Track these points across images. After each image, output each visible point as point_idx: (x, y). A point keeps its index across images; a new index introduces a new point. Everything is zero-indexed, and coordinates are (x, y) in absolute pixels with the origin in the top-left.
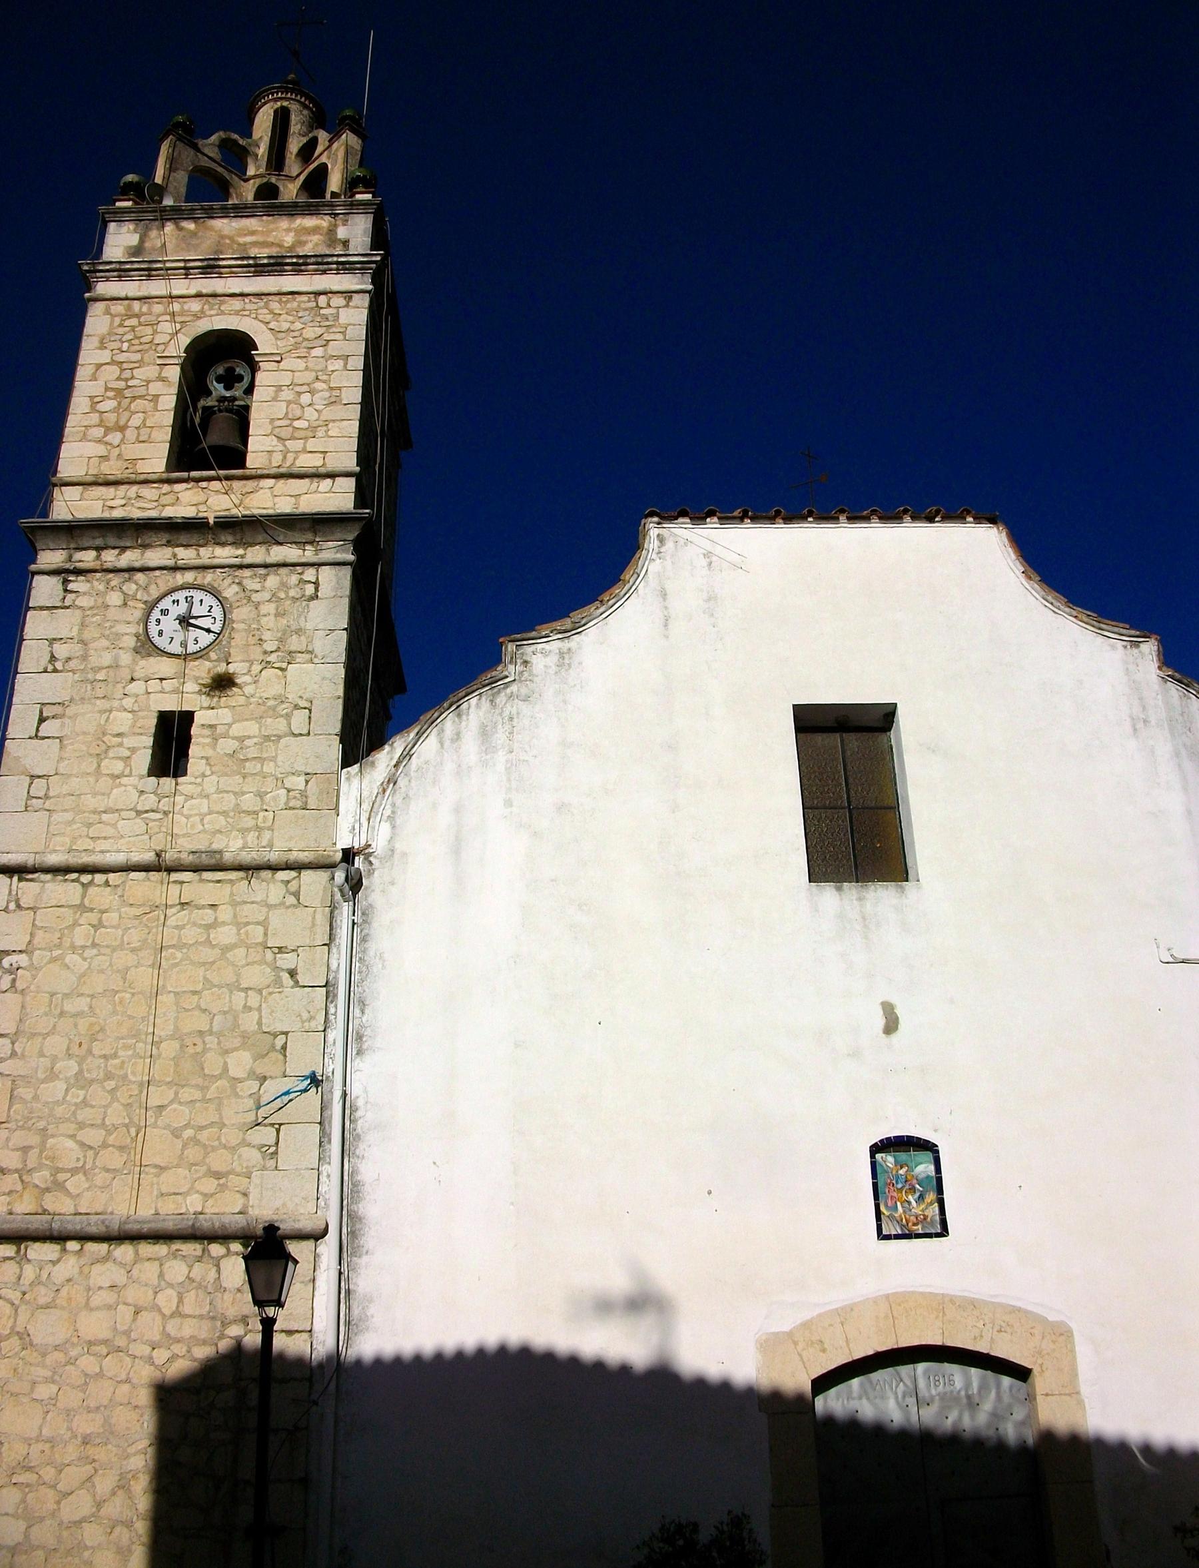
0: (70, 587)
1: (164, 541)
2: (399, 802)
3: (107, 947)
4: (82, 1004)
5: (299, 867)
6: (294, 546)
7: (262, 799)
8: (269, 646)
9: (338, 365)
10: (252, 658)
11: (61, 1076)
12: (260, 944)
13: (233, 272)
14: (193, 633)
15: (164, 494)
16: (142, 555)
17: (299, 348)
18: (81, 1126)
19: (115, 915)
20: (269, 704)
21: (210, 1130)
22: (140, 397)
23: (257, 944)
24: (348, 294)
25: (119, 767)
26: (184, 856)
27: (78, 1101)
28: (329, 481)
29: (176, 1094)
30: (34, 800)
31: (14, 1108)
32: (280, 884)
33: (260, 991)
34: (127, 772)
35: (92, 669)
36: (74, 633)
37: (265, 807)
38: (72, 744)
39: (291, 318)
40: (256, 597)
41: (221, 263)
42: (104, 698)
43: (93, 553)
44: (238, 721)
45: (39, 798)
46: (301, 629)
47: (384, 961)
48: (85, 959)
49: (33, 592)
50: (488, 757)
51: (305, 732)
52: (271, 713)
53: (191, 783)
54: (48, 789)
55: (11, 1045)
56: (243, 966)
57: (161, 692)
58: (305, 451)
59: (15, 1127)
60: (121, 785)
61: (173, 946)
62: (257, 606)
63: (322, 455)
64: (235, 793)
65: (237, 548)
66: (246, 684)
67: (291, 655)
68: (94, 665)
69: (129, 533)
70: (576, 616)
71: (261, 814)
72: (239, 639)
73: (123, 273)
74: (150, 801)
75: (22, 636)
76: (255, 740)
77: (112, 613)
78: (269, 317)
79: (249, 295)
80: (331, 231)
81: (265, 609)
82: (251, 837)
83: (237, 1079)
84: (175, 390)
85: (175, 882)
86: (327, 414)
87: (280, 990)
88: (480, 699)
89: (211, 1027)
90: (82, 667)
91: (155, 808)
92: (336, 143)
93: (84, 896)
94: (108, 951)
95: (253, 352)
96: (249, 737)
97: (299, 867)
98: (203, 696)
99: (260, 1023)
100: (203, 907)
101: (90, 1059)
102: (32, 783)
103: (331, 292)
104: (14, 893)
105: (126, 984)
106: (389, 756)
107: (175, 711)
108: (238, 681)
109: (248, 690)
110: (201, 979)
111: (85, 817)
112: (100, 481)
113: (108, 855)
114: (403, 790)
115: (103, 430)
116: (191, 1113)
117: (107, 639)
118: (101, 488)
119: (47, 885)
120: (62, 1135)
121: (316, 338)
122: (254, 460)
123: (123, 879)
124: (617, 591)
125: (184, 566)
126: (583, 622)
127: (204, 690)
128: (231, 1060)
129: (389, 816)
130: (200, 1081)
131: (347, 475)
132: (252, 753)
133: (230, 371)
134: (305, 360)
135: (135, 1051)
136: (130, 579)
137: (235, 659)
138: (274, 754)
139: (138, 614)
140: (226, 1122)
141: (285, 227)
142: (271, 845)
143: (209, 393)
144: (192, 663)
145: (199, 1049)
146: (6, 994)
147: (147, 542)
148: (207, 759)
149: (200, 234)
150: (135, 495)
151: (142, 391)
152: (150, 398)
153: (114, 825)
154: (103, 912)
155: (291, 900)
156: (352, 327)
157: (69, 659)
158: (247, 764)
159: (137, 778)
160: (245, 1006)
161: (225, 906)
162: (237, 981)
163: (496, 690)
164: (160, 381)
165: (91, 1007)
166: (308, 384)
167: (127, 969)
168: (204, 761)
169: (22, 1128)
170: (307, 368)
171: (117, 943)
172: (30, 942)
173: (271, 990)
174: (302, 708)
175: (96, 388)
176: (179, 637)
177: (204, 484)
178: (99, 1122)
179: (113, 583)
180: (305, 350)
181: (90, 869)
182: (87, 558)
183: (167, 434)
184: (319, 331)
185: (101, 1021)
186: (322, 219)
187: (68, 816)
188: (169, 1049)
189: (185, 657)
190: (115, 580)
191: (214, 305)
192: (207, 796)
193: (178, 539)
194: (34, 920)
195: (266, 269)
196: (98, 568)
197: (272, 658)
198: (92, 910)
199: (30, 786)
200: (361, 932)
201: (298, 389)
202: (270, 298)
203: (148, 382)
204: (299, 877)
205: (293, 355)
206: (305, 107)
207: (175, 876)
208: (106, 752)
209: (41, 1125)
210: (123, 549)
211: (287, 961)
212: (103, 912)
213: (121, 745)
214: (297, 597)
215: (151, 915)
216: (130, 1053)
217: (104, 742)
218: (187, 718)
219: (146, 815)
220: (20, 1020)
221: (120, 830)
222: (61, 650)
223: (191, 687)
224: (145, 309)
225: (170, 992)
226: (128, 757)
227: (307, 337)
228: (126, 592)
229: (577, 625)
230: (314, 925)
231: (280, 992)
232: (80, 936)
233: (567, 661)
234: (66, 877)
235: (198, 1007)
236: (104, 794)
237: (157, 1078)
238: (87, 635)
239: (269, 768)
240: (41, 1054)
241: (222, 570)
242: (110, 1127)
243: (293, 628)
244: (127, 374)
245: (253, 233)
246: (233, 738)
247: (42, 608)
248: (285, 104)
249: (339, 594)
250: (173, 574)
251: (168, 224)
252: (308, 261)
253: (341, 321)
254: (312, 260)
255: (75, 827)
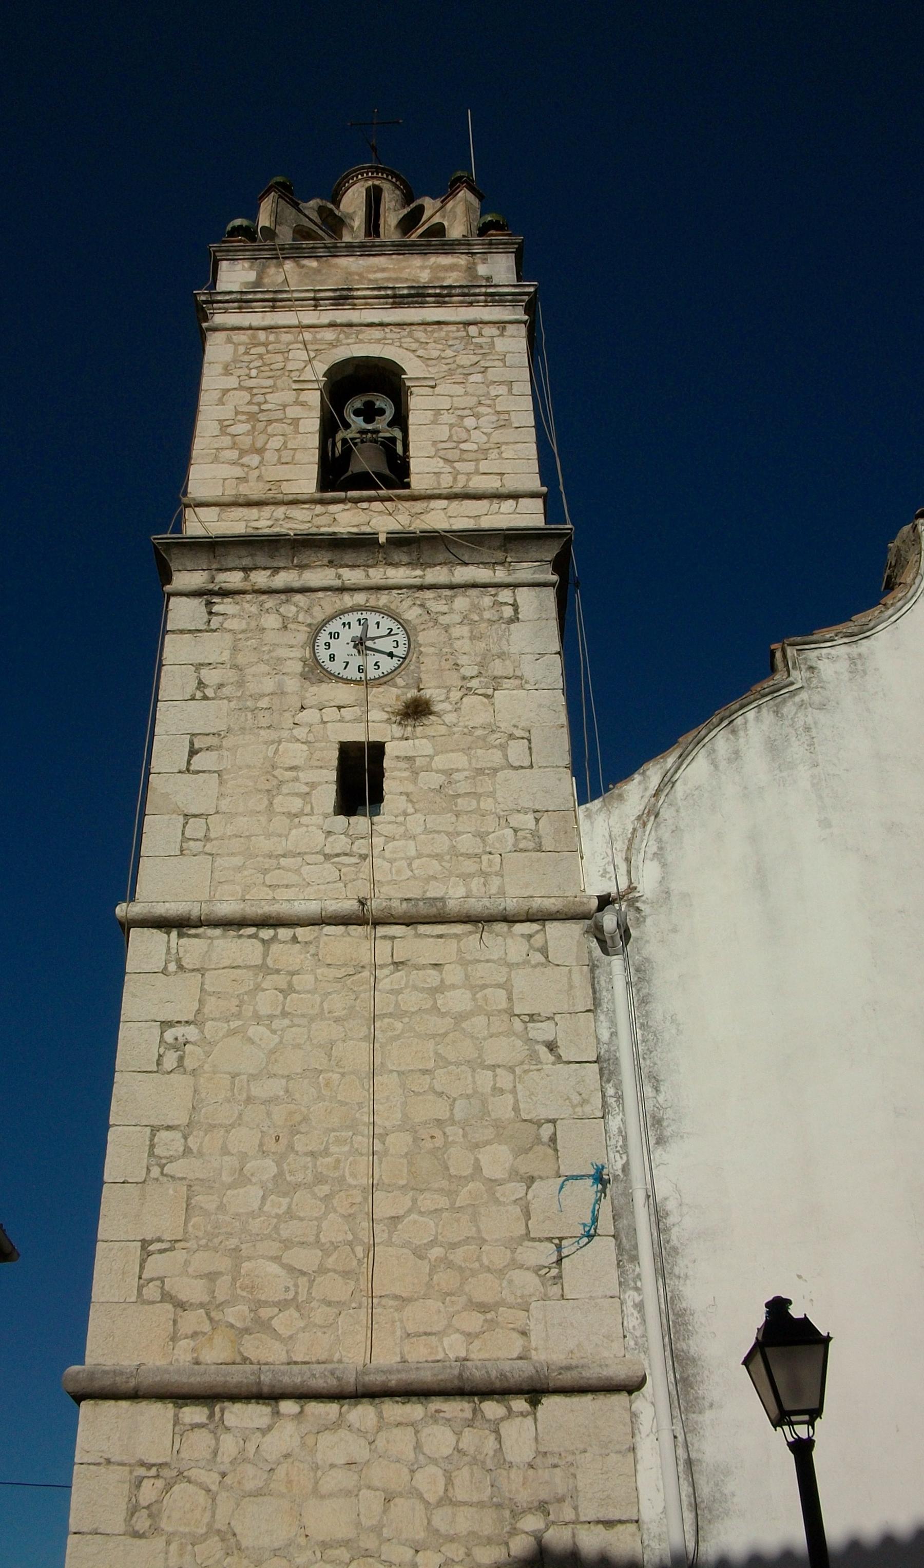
0: (215, 609)
1: (325, 561)
2: (666, 836)
3: (303, 1016)
4: (275, 1087)
5: (541, 918)
6: (481, 566)
7: (484, 841)
8: (469, 671)
9: (503, 390)
10: (448, 684)
11: (254, 1180)
12: (505, 1011)
13: (368, 302)
14: (372, 658)
15: (317, 516)
16: (300, 576)
17: (454, 374)
18: (287, 1244)
19: (310, 978)
20: (476, 734)
21: (466, 1247)
22: (276, 421)
23: (499, 1011)
24: (501, 325)
25: (296, 804)
26: (395, 904)
27: (281, 1212)
28: (511, 502)
29: (414, 1201)
30: (191, 843)
31: (194, 1220)
32: (520, 939)
33: (511, 1070)
34: (307, 809)
35: (251, 696)
36: (226, 657)
37: (488, 849)
38: (233, 779)
39: (440, 347)
40: (443, 620)
41: (355, 293)
42: (269, 728)
43: (240, 575)
44: (442, 752)
45: (197, 840)
46: (504, 653)
47: (678, 1025)
48: (274, 1032)
49: (170, 615)
50: (785, 774)
51: (526, 763)
52: (481, 743)
53: (390, 823)
54: (208, 829)
55: (183, 1141)
56: (485, 1039)
57: (339, 721)
58: (477, 472)
59: (195, 1246)
60: (300, 824)
61: (391, 1015)
62: (447, 628)
63: (499, 477)
64: (448, 834)
65: (413, 569)
66: (446, 712)
67: (497, 682)
68: (253, 692)
69: (283, 551)
70: (860, 619)
71: (485, 858)
72: (430, 663)
73: (244, 304)
74: (340, 843)
75: (161, 660)
76: (466, 773)
77: (269, 637)
78: (414, 346)
79: (390, 325)
80: (470, 268)
81: (456, 631)
82: (476, 884)
83: (495, 1180)
84: (317, 413)
85: (384, 937)
86: (497, 436)
87: (539, 1067)
88: (759, 712)
89: (452, 1114)
90: (239, 694)
91: (348, 851)
92: (451, 202)
93: (265, 955)
94: (304, 1021)
95: (403, 376)
96: (458, 770)
97: (541, 918)
98: (394, 726)
99: (516, 1109)
100: (423, 967)
101: (292, 1156)
102: (187, 823)
103: (481, 323)
104: (174, 951)
105: (333, 1063)
106: (642, 787)
107: (364, 742)
108: (437, 708)
109: (450, 718)
110: (432, 1054)
111: (259, 862)
112: (241, 500)
113: (296, 903)
114: (670, 822)
115: (238, 452)
116: (437, 1225)
117: (268, 664)
118: (241, 509)
119: (216, 942)
120: (262, 1257)
121: (471, 365)
122: (419, 480)
123: (316, 935)
124: (900, 595)
125: (353, 587)
126: (871, 624)
127: (393, 719)
128: (485, 1157)
129: (655, 854)
130: (444, 1184)
131: (533, 495)
132: (464, 787)
133: (369, 405)
134: (462, 385)
135: (352, 1146)
136: (287, 600)
137: (427, 685)
138: (492, 789)
139: (302, 636)
140: (487, 1238)
141: (418, 265)
142: (502, 892)
143: (347, 426)
144: (374, 689)
145: (439, 1142)
146: (172, 1074)
147: (305, 562)
148: (407, 795)
149: (324, 271)
150: (283, 516)
151: (279, 414)
152: (289, 421)
153: (297, 871)
154: (293, 974)
155: (538, 957)
156: (511, 355)
157: (221, 686)
158: (459, 801)
159: (321, 817)
160: (494, 1088)
161: (453, 966)
162: (478, 1058)
163: (779, 699)
164: (297, 405)
165: (287, 1091)
166: (470, 409)
167: (332, 1044)
168: (404, 798)
169: (206, 1247)
170: (466, 393)
171: (316, 1012)
172: (199, 1011)
173: (526, 1067)
174: (518, 738)
175: (226, 412)
176: (357, 660)
177: (365, 505)
178: (312, 1239)
179: (267, 606)
180: (462, 376)
181: (271, 921)
182: (234, 579)
183: (314, 455)
184: (475, 359)
185: (303, 1109)
186: (458, 257)
187: (237, 861)
188: (399, 1142)
189: (367, 683)
190: (270, 602)
191: (351, 334)
192: (413, 837)
193: (342, 559)
194: (203, 984)
195: (406, 300)
196: (248, 588)
197: (474, 683)
198: (278, 971)
199: (184, 827)
200: (638, 991)
201: (460, 412)
202: (414, 328)
203: (285, 406)
204: (543, 929)
205: (449, 381)
206: (397, 187)
207: (381, 930)
208: (279, 787)
209: (233, 1243)
210: (276, 570)
211: (543, 1031)
212: (293, 974)
213: (296, 779)
214: (494, 619)
215: (355, 978)
216: (346, 1148)
217: (274, 776)
218: (378, 750)
219: (336, 859)
220: (193, 1107)
221: (305, 876)
222: (211, 677)
223: (376, 715)
224: (272, 338)
225: (391, 1071)
226: (308, 793)
227: (462, 364)
228: (285, 614)
229: (865, 628)
230: (571, 987)
231: (538, 1070)
232: (265, 1002)
233: (860, 667)
234: (241, 932)
235: (432, 1089)
236: (280, 836)
237: (386, 1181)
238: (241, 659)
239: (487, 804)
240: (225, 1151)
241: (400, 592)
242: (328, 1245)
243: (494, 652)
244: (260, 398)
245: (383, 270)
246: (437, 772)
247: (182, 632)
248: (377, 182)
249: (544, 616)
250: (340, 596)
251: (287, 262)
252: (453, 291)
253: (497, 349)
254: (458, 291)
255: (246, 873)
